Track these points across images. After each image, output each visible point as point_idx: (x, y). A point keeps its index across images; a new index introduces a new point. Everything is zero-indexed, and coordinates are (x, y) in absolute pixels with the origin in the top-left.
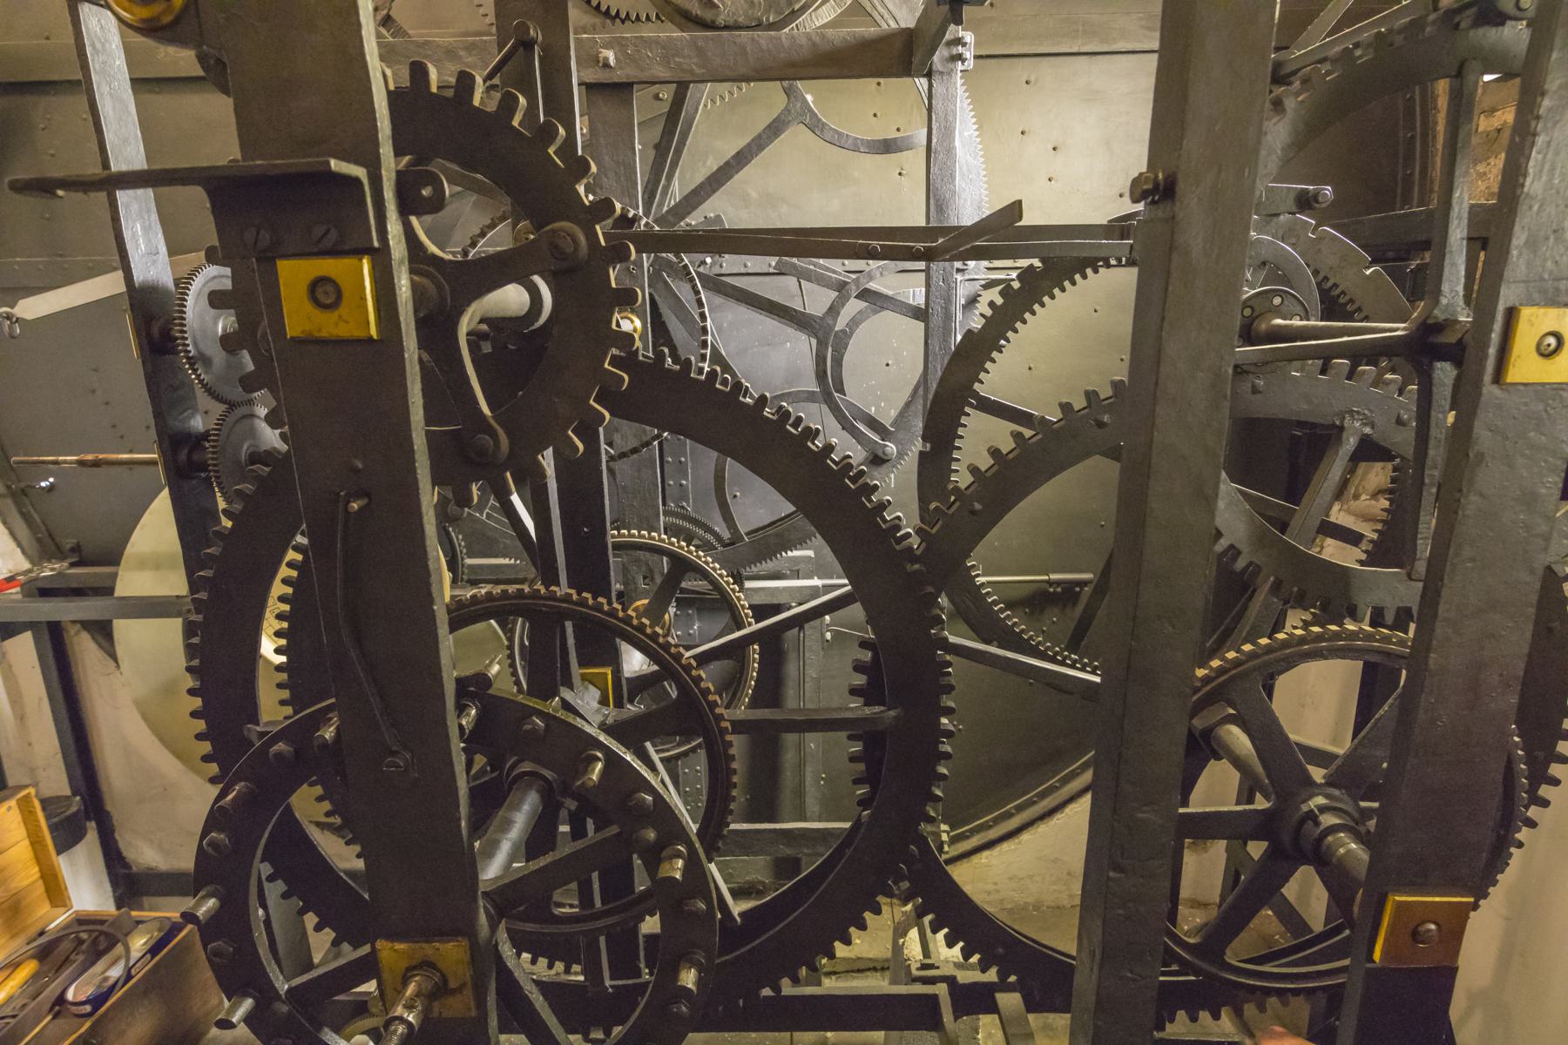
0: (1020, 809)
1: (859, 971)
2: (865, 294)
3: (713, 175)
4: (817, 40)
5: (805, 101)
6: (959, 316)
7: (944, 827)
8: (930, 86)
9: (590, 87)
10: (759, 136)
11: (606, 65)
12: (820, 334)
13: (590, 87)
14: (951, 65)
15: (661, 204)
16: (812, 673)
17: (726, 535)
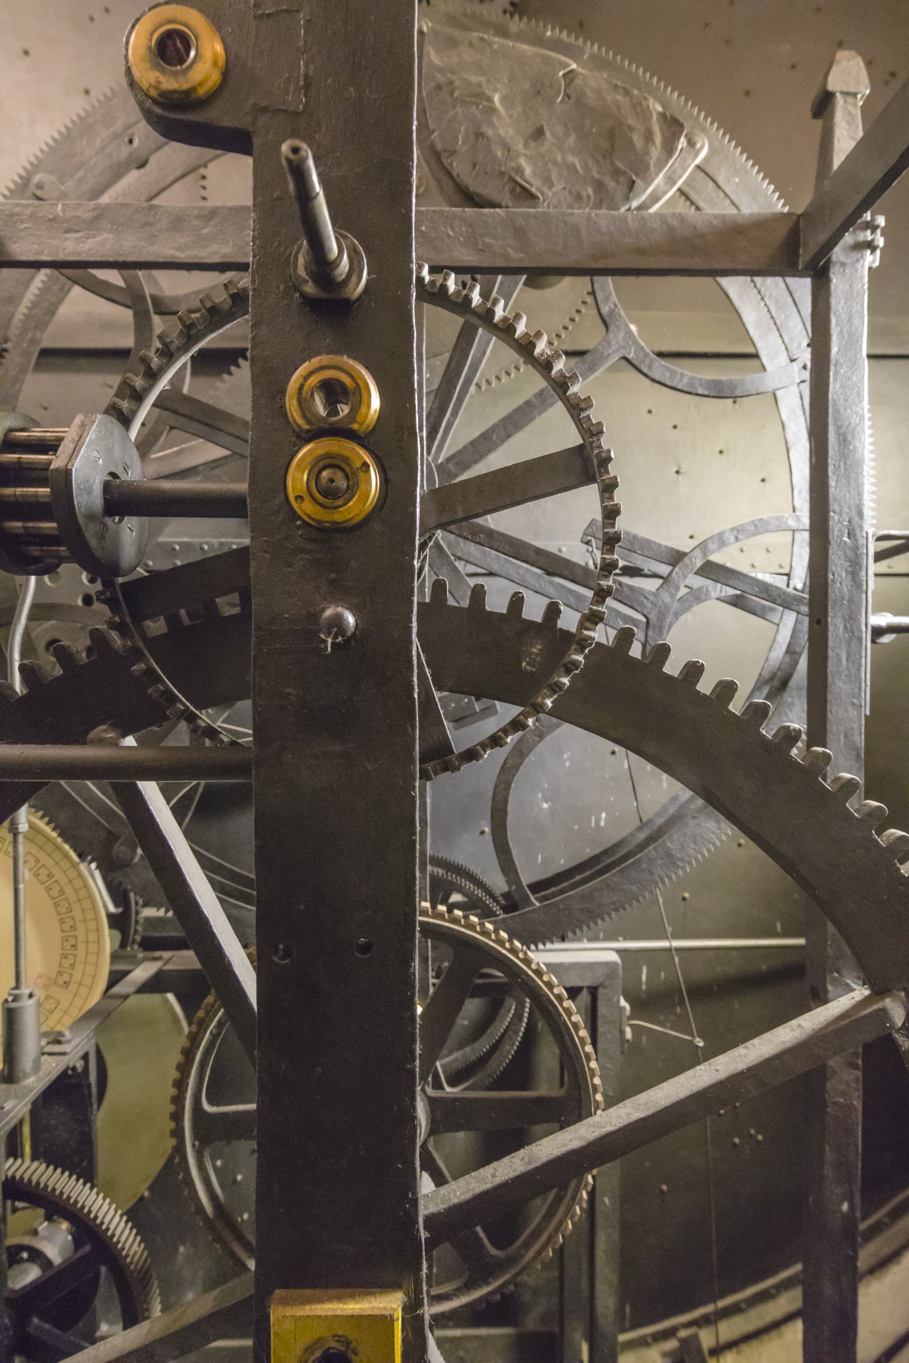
3: (509, 417)
4: (675, 223)
5: (629, 332)
12: (653, 616)
14: (856, 255)
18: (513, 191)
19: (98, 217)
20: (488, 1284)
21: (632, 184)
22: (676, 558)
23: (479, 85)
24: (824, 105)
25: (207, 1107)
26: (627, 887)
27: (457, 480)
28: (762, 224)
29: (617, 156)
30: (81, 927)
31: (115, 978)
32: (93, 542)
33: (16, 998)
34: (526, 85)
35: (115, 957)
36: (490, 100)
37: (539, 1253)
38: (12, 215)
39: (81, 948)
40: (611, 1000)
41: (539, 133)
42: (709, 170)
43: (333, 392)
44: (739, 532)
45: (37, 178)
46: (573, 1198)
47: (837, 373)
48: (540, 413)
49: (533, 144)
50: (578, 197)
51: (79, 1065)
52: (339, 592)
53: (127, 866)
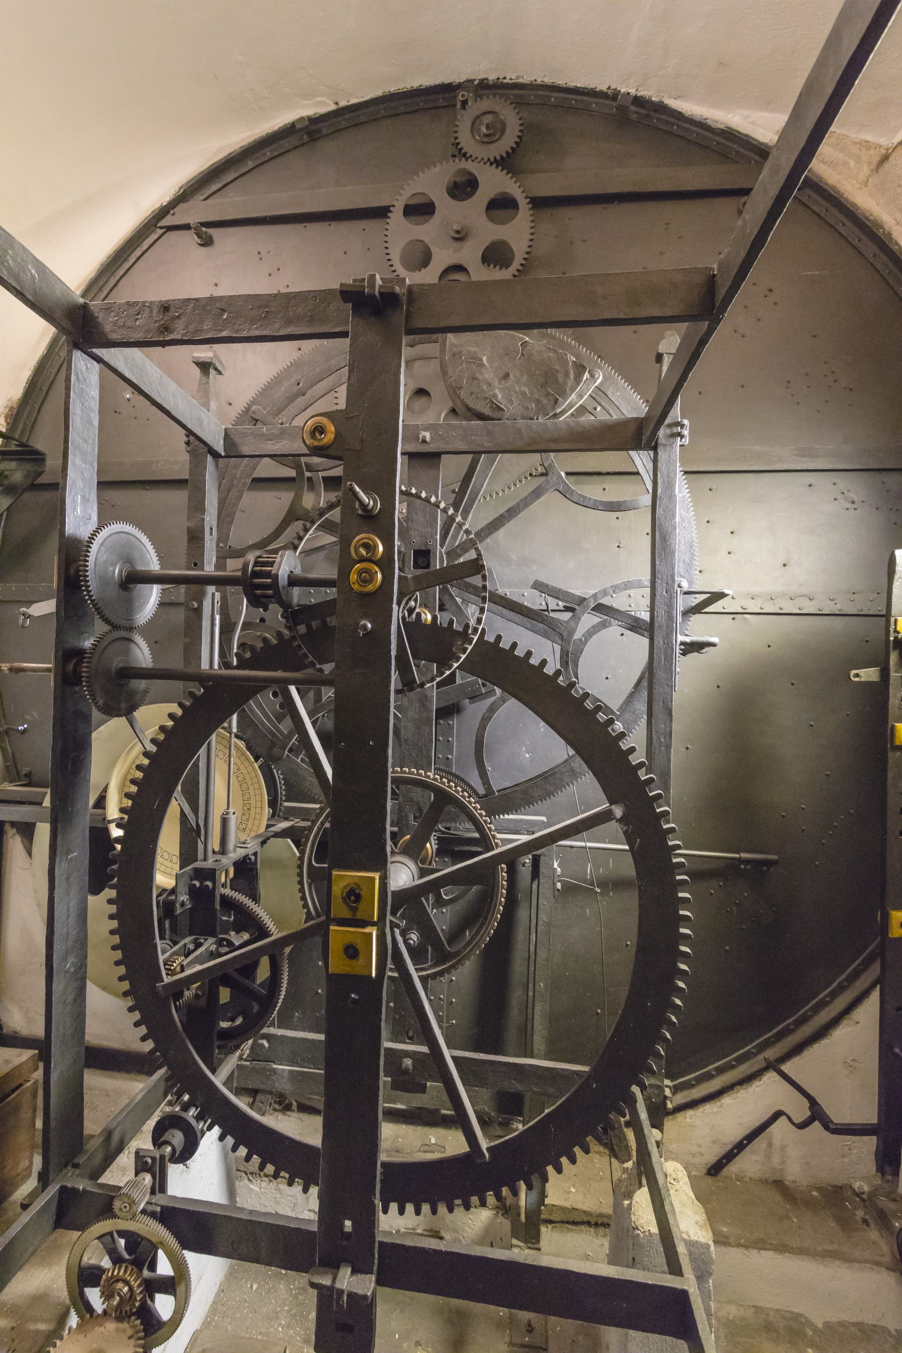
0: (721, 1071)
1: (574, 1223)
2: (600, 608)
3: (491, 523)
4: (573, 425)
6: (679, 619)
7: (667, 1082)
8: (655, 461)
9: (411, 456)
10: (526, 498)
11: (424, 441)
12: (565, 634)
13: (411, 456)
14: (672, 440)
15: (455, 537)
16: (543, 917)
17: (481, 791)
18: (491, 407)
19: (282, 433)
20: (445, 964)
21: (556, 400)
22: (582, 600)
23: (475, 352)
24: (659, 358)
25: (314, 863)
26: (547, 787)
27: (462, 560)
28: (623, 424)
29: (551, 383)
30: (253, 798)
31: (268, 826)
32: (284, 598)
33: (227, 813)
34: (501, 351)
35: (269, 819)
36: (481, 360)
37: (471, 950)
38: (243, 433)
39: (253, 810)
40: (548, 864)
41: (506, 376)
42: (603, 389)
43: (366, 546)
44: (616, 589)
45: (254, 408)
46: (489, 923)
47: (661, 503)
48: (508, 521)
49: (503, 382)
50: (527, 408)
51: (253, 858)
52: (366, 616)
53: (280, 759)
